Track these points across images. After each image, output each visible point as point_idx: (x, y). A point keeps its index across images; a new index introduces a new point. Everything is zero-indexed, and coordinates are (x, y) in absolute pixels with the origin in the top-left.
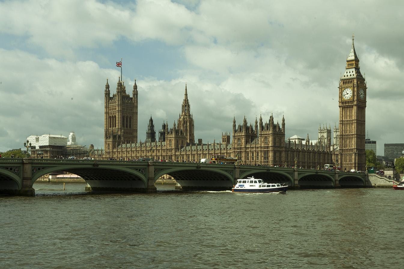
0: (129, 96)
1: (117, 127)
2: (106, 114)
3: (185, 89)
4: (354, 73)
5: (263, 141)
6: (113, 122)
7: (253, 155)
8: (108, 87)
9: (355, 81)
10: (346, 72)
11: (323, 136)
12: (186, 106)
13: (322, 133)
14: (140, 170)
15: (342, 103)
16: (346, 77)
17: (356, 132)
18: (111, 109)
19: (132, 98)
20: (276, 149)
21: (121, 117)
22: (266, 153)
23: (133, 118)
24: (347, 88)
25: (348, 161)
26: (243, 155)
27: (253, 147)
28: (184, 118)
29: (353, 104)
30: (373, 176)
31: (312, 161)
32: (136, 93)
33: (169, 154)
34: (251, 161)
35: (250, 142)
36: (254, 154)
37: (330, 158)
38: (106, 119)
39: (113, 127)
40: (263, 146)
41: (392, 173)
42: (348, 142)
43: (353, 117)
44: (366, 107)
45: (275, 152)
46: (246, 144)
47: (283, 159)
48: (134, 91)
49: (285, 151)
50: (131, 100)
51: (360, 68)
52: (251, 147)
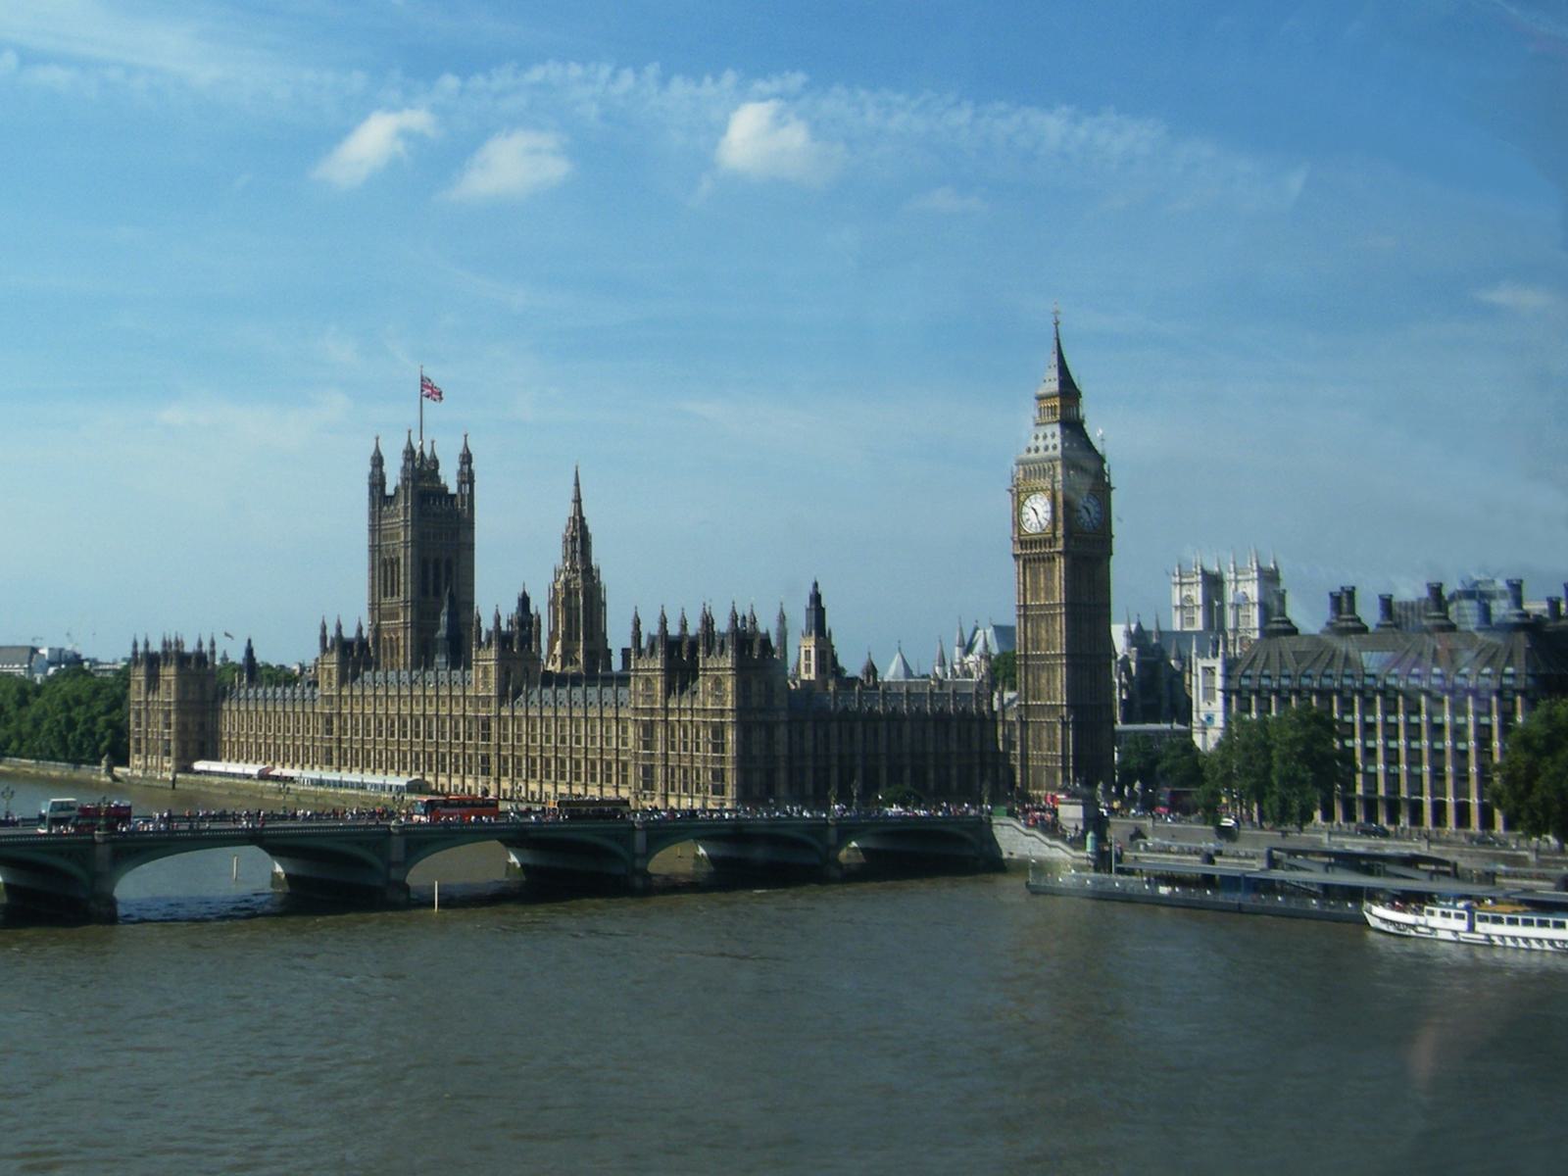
0: (446, 489)
1: (402, 595)
4: (1058, 441)
6: (393, 580)
7: (685, 735)
8: (378, 461)
9: (1059, 470)
10: (1033, 436)
11: (1189, 599)
12: (574, 539)
13: (1185, 588)
15: (1023, 544)
16: (1033, 455)
17: (1064, 647)
19: (455, 496)
22: (718, 731)
24: (1035, 491)
25: (1045, 746)
27: (685, 710)
28: (567, 582)
29: (1052, 550)
30: (1006, 827)
32: (467, 478)
34: (679, 755)
35: (677, 691)
36: (689, 732)
38: (373, 568)
39: (392, 595)
40: (709, 707)
41: (1081, 816)
42: (1044, 681)
43: (1057, 594)
45: (744, 728)
46: (667, 696)
48: (461, 473)
50: (452, 501)
51: (1086, 420)
52: (679, 709)
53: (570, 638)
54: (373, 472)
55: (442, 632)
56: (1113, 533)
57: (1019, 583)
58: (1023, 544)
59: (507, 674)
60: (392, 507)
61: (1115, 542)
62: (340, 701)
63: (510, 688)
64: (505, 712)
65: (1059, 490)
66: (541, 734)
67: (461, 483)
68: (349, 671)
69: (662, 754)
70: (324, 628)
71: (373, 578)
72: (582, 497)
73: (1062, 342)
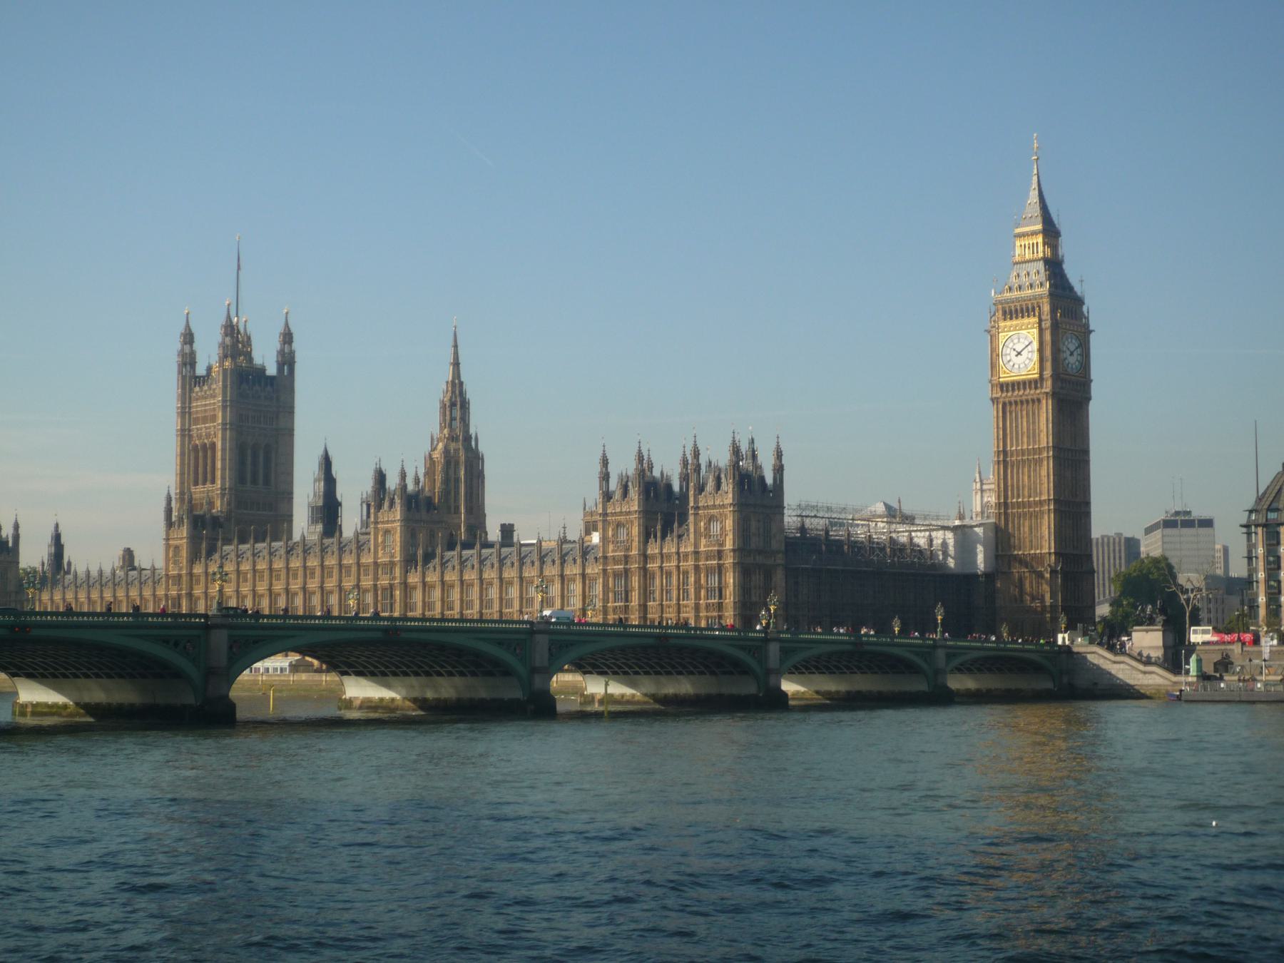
1: (219, 482)
2: (183, 436)
3: (451, 343)
5: (702, 530)
8: (188, 338)
9: (1046, 308)
12: (453, 405)
14: (176, 644)
16: (1015, 294)
17: (1052, 492)
18: (198, 418)
28: (446, 451)
32: (287, 360)
33: (384, 582)
35: (659, 534)
38: (182, 454)
39: (204, 483)
41: (1161, 644)
42: (1027, 529)
44: (1089, 399)
45: (745, 570)
46: (646, 542)
48: (281, 353)
50: (272, 385)
54: (182, 350)
56: (1092, 377)
57: (998, 428)
58: (1004, 387)
60: (206, 388)
61: (1095, 389)
62: (191, 580)
65: (1046, 329)
67: (280, 366)
69: (640, 605)
71: (182, 464)
72: (460, 361)
73: (1041, 178)
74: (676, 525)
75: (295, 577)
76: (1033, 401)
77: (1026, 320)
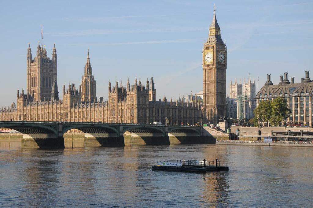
0: (49, 58)
1: (37, 86)
3: (87, 53)
7: (123, 112)
8: (30, 50)
9: (215, 47)
12: (88, 69)
16: (209, 43)
17: (215, 90)
20: (140, 107)
21: (41, 78)
23: (52, 78)
24: (208, 52)
26: (116, 111)
28: (86, 79)
31: (177, 116)
32: (55, 56)
33: (66, 111)
37: (196, 113)
39: (34, 87)
41: (224, 126)
44: (226, 68)
45: (139, 109)
46: (118, 102)
47: (148, 115)
48: (53, 54)
49: (149, 108)
50: (51, 63)
53: (86, 94)
55: (53, 92)
58: (205, 66)
59: (72, 100)
60: (34, 63)
62: (23, 111)
63: (74, 104)
64: (72, 110)
66: (82, 115)
68: (26, 103)
70: (18, 91)
74: (124, 99)
75: (47, 110)
76: (212, 69)
77: (210, 50)
